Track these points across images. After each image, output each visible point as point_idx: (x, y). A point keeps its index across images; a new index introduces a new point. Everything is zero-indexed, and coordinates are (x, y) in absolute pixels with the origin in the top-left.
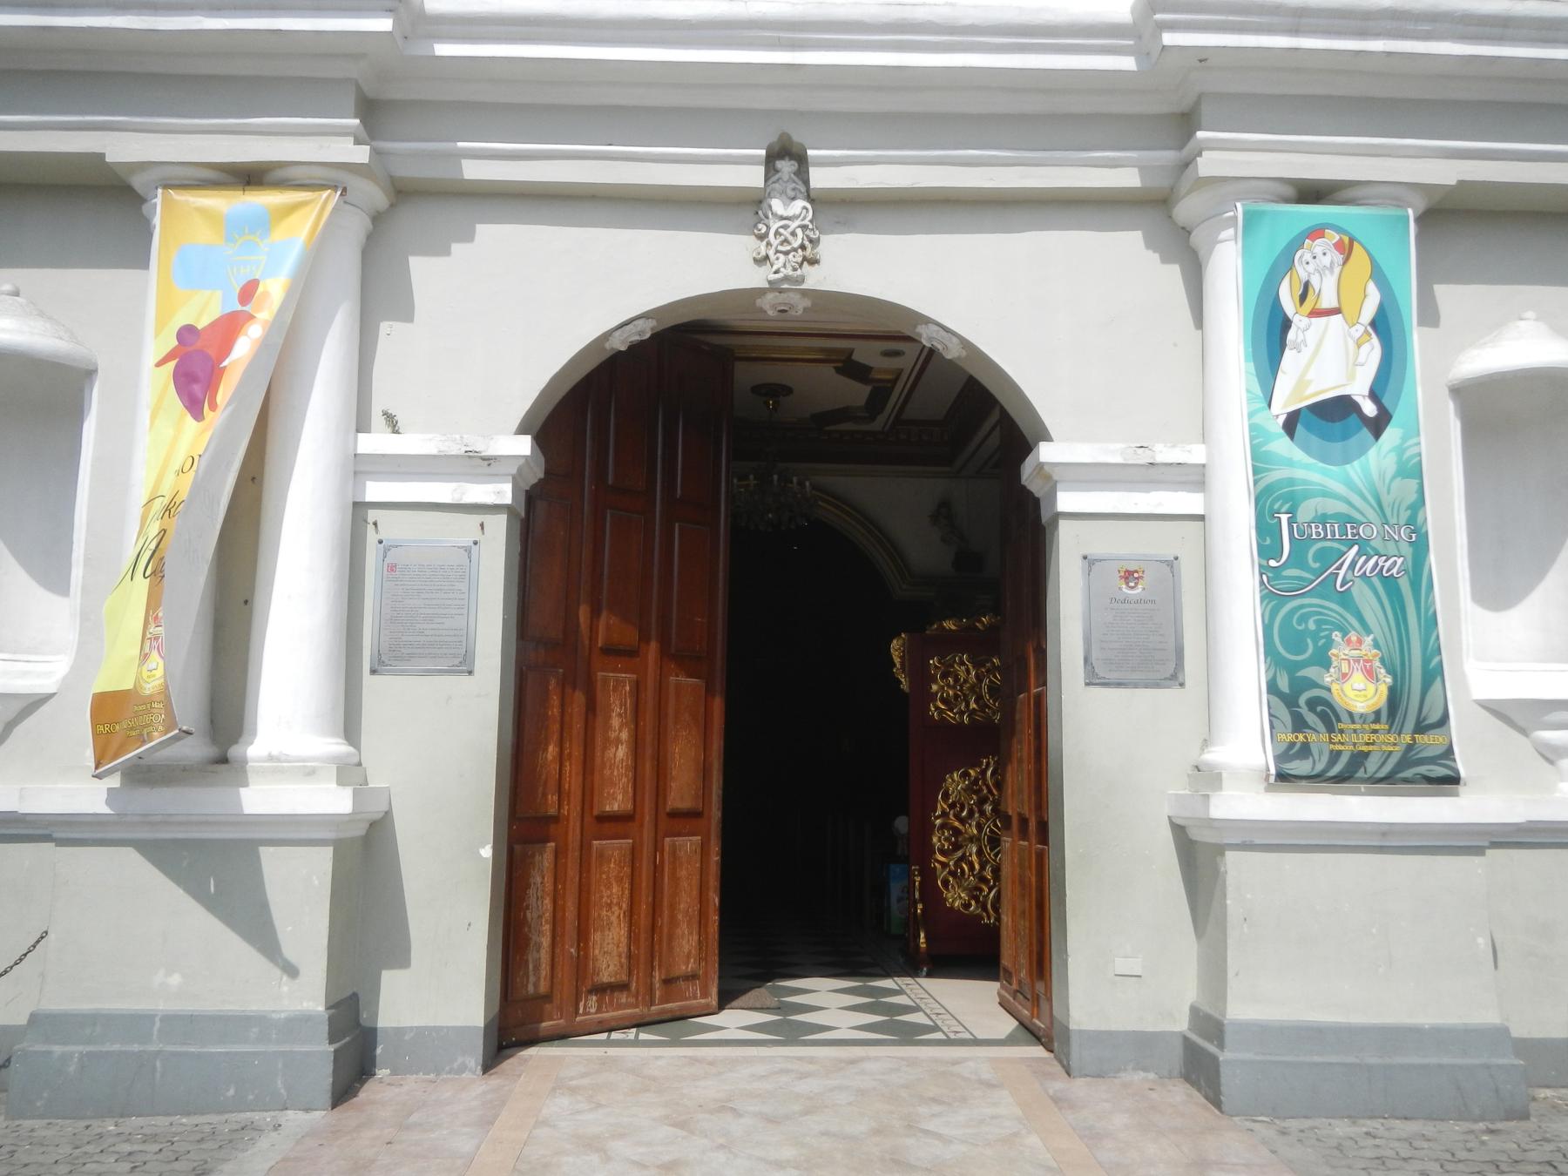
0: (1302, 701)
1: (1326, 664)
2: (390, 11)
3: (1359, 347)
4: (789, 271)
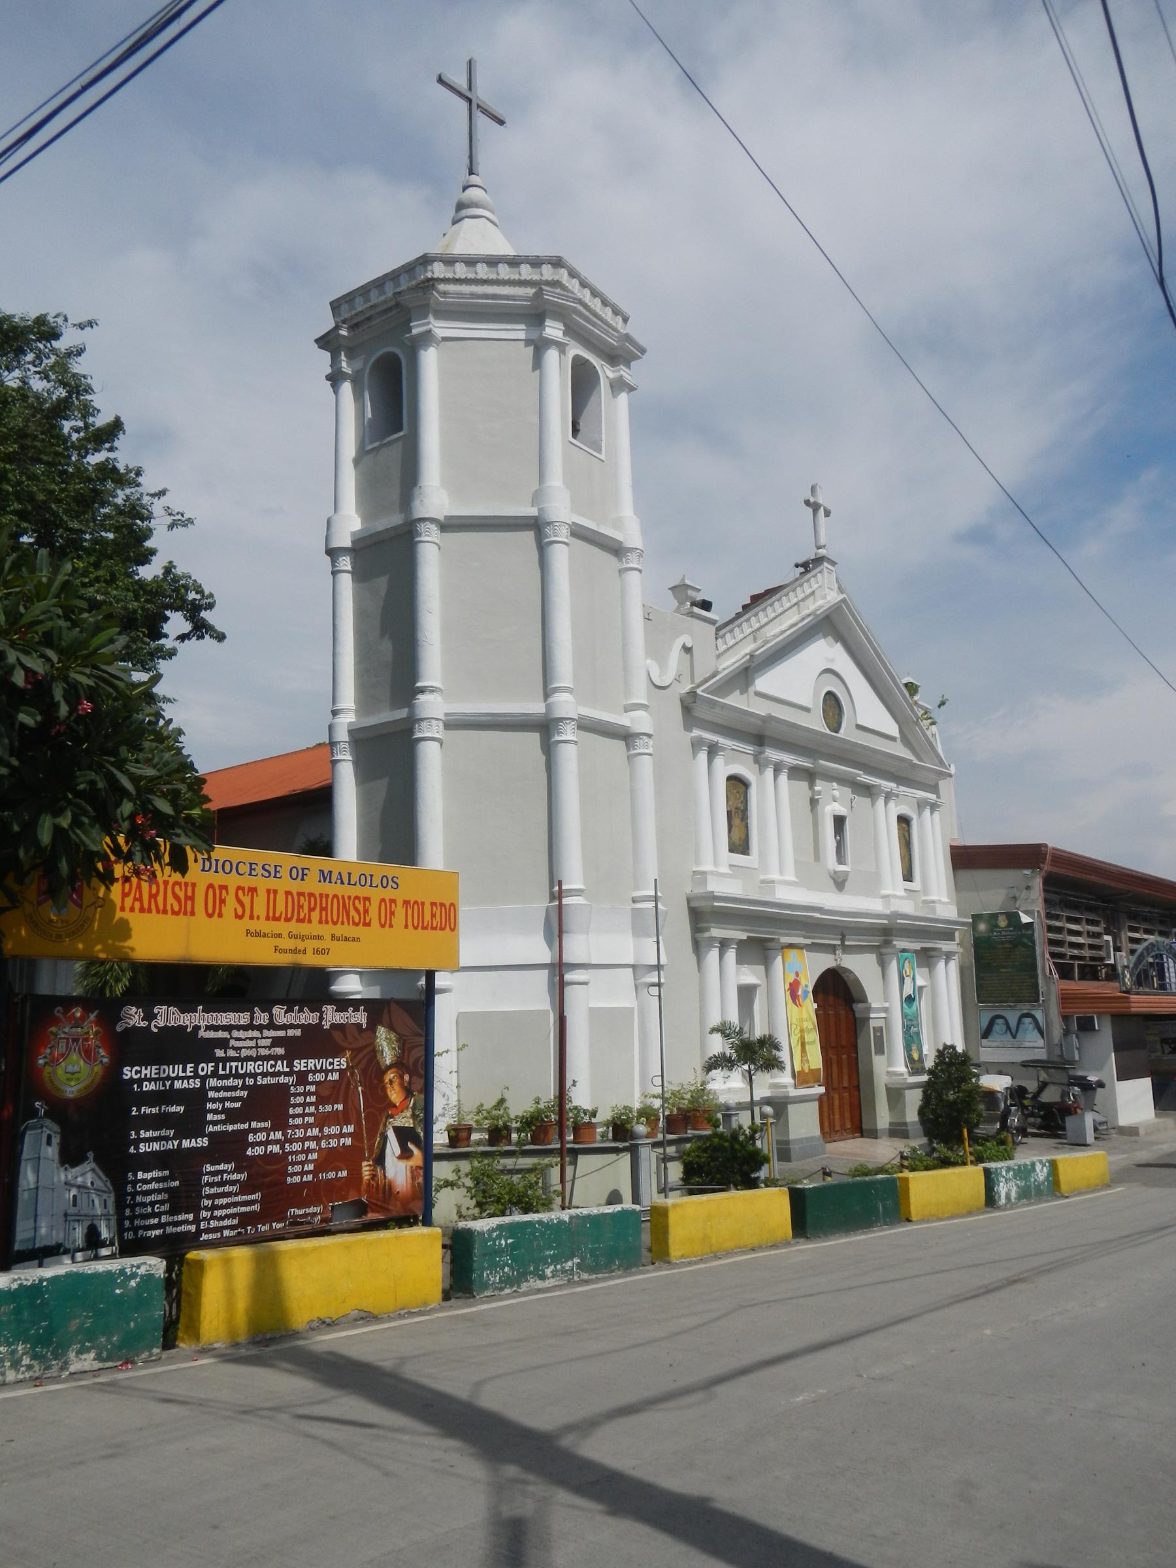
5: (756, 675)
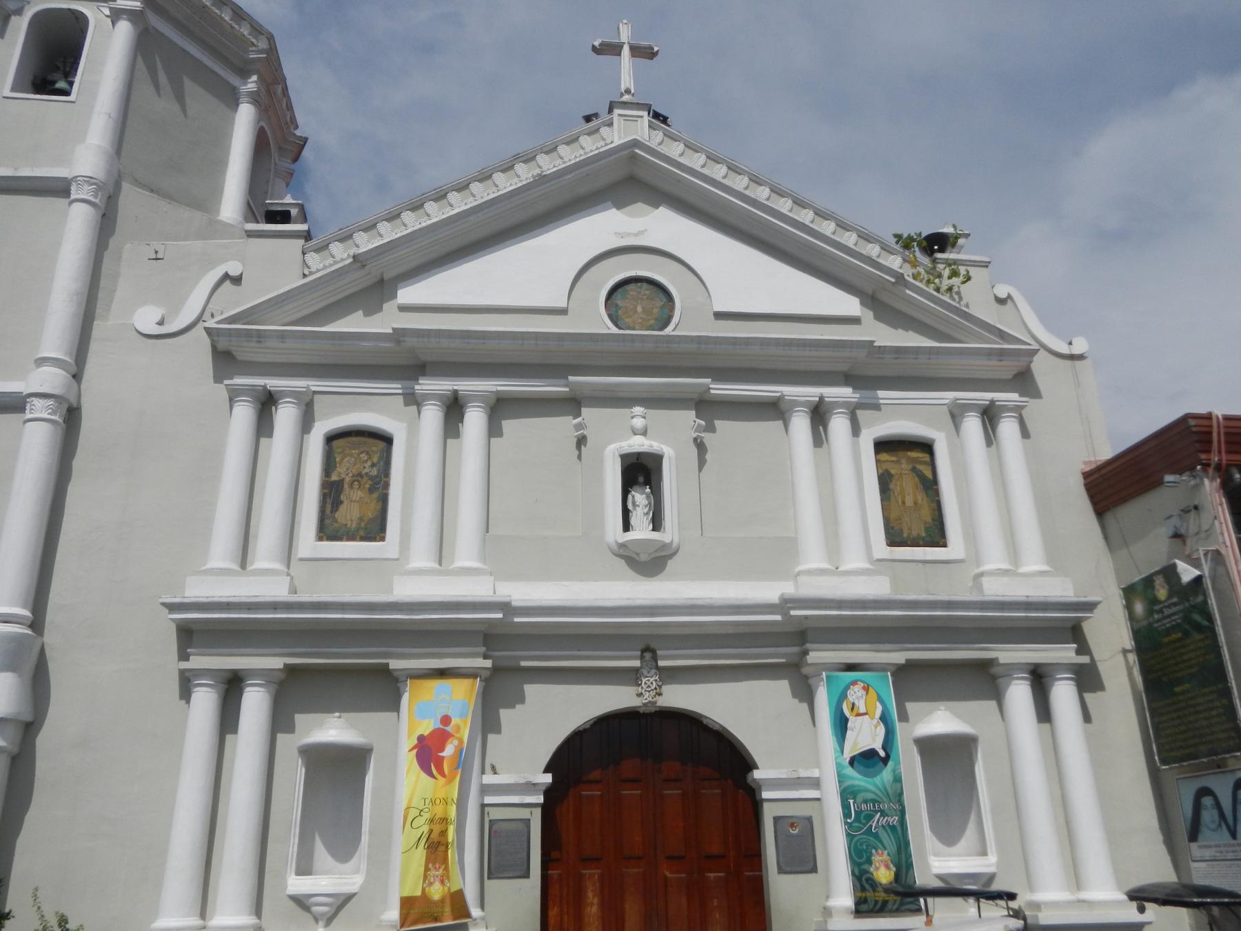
0: (863, 879)
1: (870, 862)
2: (501, 609)
3: (876, 727)
4: (650, 699)
5: (399, 285)
